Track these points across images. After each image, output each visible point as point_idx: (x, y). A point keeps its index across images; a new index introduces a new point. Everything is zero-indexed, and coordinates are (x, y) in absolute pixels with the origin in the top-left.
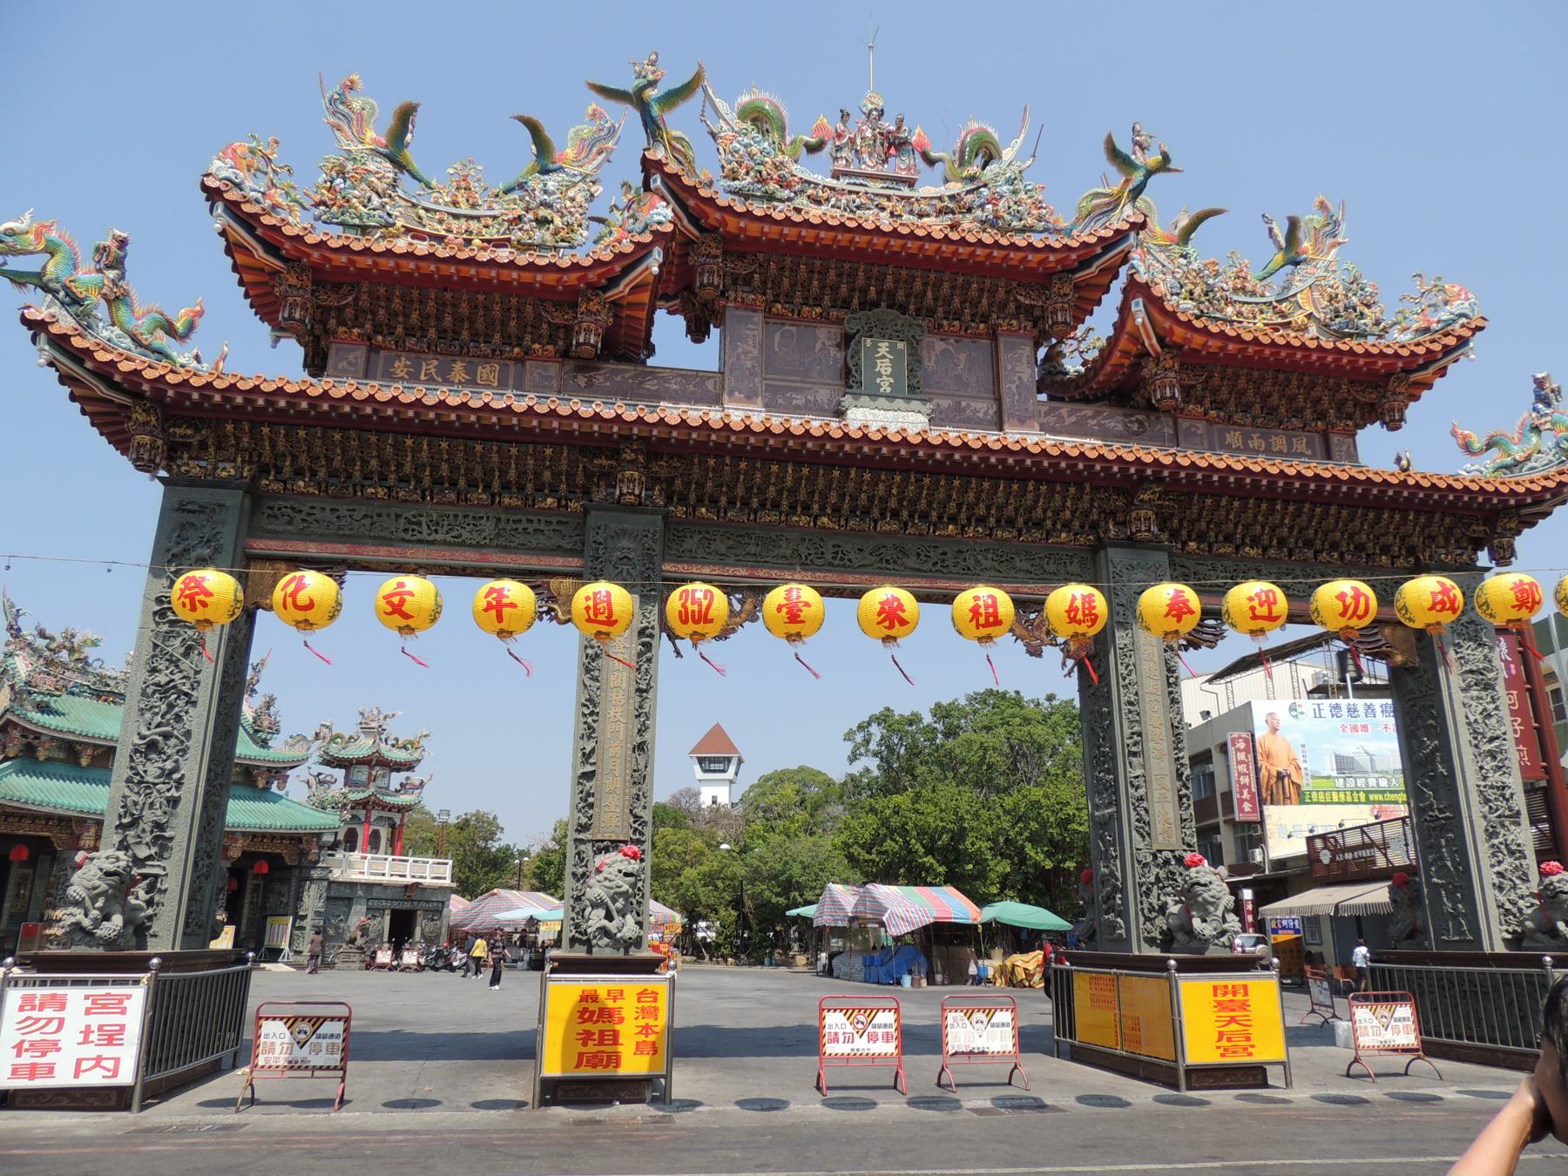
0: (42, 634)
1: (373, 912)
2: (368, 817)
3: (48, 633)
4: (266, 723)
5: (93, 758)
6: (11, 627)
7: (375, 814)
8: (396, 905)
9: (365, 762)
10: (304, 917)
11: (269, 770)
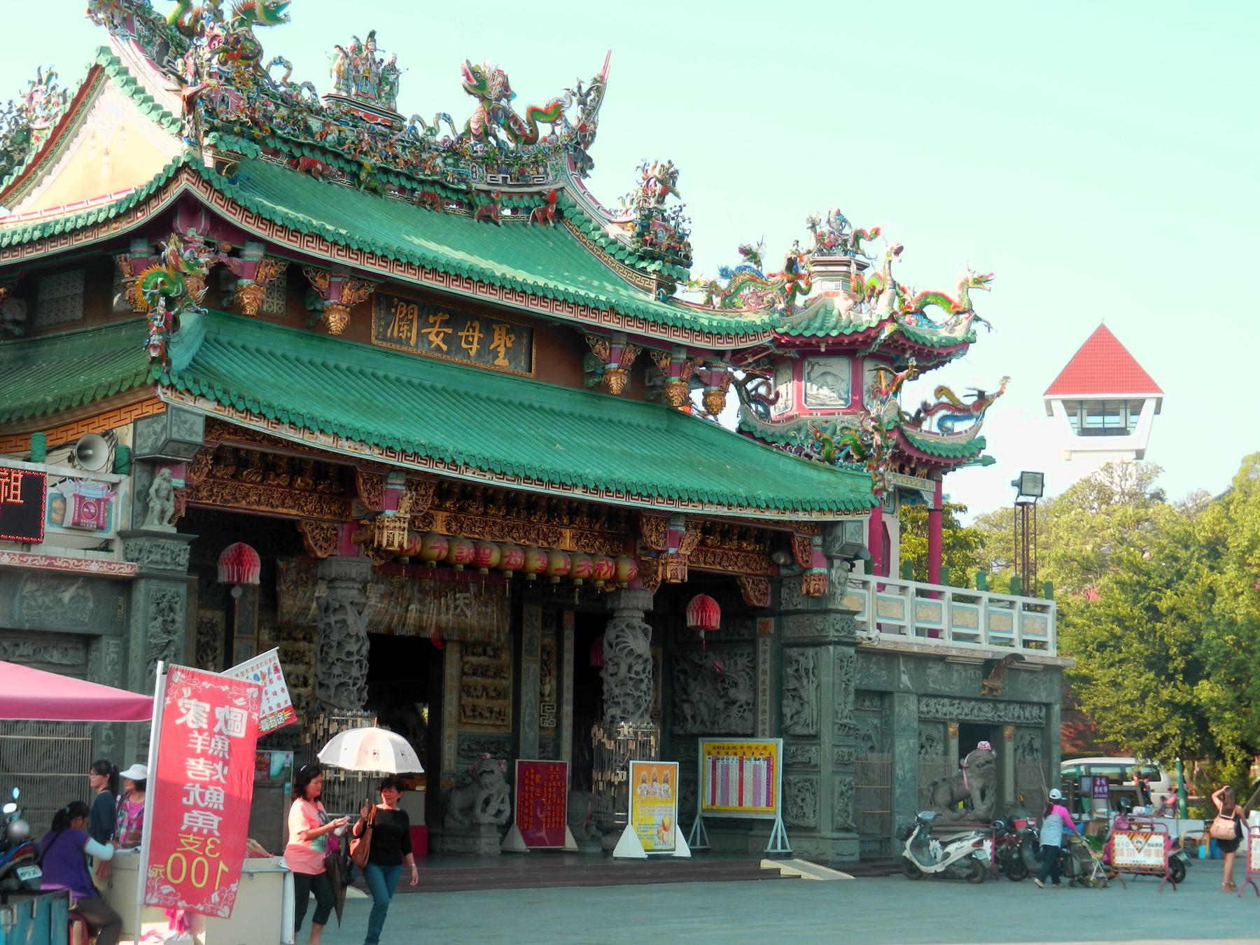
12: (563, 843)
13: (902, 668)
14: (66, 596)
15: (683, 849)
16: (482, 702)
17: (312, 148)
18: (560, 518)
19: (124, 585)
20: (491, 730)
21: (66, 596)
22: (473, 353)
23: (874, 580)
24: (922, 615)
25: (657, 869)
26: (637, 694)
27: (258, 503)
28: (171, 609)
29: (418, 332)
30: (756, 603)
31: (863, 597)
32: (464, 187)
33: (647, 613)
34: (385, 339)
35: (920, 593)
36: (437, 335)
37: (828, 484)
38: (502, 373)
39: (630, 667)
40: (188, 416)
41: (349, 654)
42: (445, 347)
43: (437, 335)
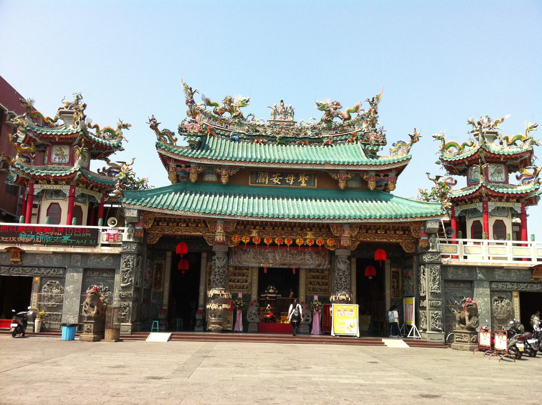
0: (208, 103)
1: (498, 294)
2: (485, 209)
3: (212, 101)
4: (372, 138)
5: (230, 177)
6: (187, 102)
7: (492, 205)
9: (473, 161)
10: (424, 298)
13: (478, 271)
14: (104, 259)
15: (358, 335)
16: (317, 286)
18: (306, 229)
19: (119, 256)
20: (323, 295)
21: (104, 259)
22: (291, 184)
23: (461, 241)
26: (340, 282)
28: (128, 261)
30: (407, 251)
31: (457, 247)
32: (317, 137)
34: (256, 183)
36: (276, 180)
37: (426, 208)
38: (303, 188)
41: (216, 272)
42: (280, 183)
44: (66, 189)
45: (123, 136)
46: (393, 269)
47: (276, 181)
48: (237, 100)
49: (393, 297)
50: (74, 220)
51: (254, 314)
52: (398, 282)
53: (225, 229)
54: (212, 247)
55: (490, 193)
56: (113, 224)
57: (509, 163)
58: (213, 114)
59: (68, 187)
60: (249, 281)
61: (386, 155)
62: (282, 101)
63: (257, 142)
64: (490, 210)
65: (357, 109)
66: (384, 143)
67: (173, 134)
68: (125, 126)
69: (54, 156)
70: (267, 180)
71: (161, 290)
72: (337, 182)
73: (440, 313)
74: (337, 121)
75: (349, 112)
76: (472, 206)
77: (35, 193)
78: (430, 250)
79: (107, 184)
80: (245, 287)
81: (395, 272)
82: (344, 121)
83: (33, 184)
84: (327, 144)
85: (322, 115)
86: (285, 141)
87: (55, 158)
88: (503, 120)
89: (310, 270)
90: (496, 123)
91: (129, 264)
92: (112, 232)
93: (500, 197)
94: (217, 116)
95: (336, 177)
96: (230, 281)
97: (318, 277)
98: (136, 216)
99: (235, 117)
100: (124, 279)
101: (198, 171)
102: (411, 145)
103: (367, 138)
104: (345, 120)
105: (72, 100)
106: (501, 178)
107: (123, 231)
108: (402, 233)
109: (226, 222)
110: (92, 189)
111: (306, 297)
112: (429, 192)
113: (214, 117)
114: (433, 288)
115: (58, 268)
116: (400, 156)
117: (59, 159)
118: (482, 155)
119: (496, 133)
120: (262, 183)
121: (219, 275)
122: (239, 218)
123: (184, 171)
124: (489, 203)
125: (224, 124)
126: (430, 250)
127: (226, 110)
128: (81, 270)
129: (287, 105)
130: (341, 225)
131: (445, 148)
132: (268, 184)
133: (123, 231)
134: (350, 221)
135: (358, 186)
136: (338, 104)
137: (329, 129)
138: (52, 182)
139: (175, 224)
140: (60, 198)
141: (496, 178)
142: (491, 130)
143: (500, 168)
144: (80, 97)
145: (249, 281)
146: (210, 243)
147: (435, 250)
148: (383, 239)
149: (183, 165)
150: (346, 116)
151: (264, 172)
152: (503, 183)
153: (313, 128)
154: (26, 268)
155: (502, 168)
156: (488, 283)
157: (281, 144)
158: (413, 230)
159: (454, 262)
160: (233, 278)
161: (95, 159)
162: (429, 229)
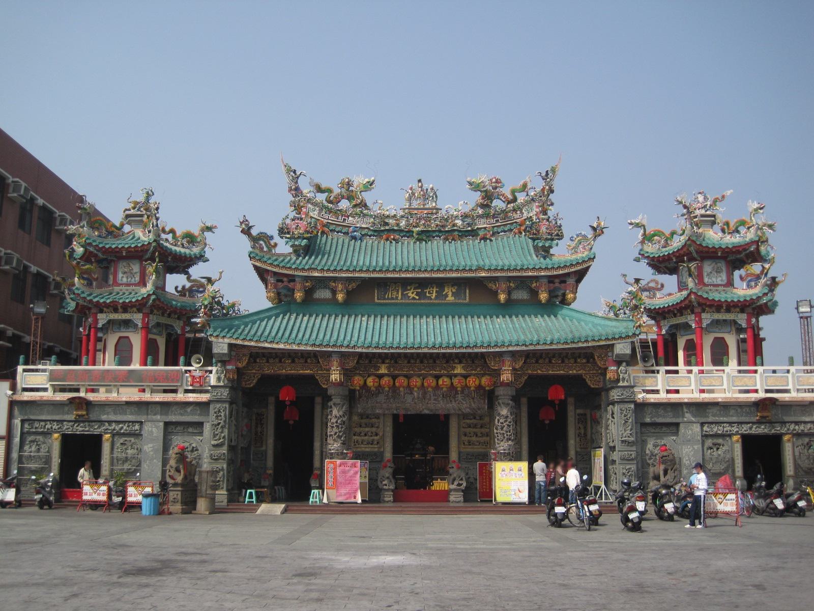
0: (319, 189)
2: (699, 322)
3: (323, 186)
4: (543, 229)
5: (349, 294)
6: (290, 190)
8: (745, 430)
11: (551, 279)
12: (700, 496)
13: (685, 410)
16: (474, 439)
17: (388, 231)
18: (453, 360)
22: (433, 298)
24: (705, 382)
25: (511, 508)
27: (291, 370)
28: (219, 411)
29: (402, 294)
30: (592, 386)
32: (470, 229)
33: (513, 396)
34: (385, 299)
35: (668, 372)
36: (413, 293)
37: (615, 327)
39: (499, 421)
40: (221, 344)
43: (413, 293)
44: (138, 318)
45: (208, 242)
46: (578, 411)
47: (411, 294)
48: (359, 180)
49: (578, 450)
50: (149, 359)
51: (388, 478)
52: (585, 428)
53: (342, 365)
54: (326, 389)
55: (704, 302)
56: (199, 363)
57: (731, 258)
58: (326, 204)
59: (140, 316)
60: (381, 434)
61: (562, 253)
62: (420, 181)
63: (387, 239)
64: (704, 325)
65: (524, 187)
66: (560, 237)
67: (272, 238)
68: (209, 229)
69: (120, 275)
70: (400, 294)
71: (264, 448)
72: (496, 294)
73: (634, 467)
74: (498, 204)
75: (513, 192)
76: (680, 320)
77: (100, 325)
78: (621, 384)
79: (188, 309)
80: (376, 443)
81: (582, 414)
82: (508, 203)
83: (96, 314)
84: (484, 239)
85: (477, 197)
86: (426, 236)
87: (122, 277)
88: (723, 197)
89: (465, 416)
90: (715, 202)
91: (221, 416)
92: (197, 374)
93: (718, 306)
94: (330, 205)
95: (494, 287)
96: (354, 435)
97: (475, 426)
98: (226, 351)
99: (355, 206)
100: (215, 435)
101: (305, 287)
102: (594, 240)
103: (536, 230)
104: (509, 202)
105: (141, 198)
106: (722, 278)
107: (211, 372)
108: (584, 361)
109: (344, 356)
110: (169, 316)
111: (460, 453)
112: (618, 304)
113: (326, 208)
114: (624, 435)
115: (133, 422)
116: (582, 255)
117: (127, 278)
118: (692, 249)
119: (714, 216)
120: (392, 299)
121: (337, 427)
122: (360, 350)
123: (286, 288)
124: (704, 315)
125: (340, 217)
126: (621, 384)
127: (343, 197)
128: (162, 424)
129: (428, 186)
130: (501, 354)
131: (647, 238)
132: (402, 299)
133: (211, 372)
134: (511, 349)
135: (525, 297)
136: (498, 181)
137: (486, 216)
138: (120, 310)
139: (277, 360)
140: (131, 329)
141: (714, 279)
142: (708, 213)
143: (719, 265)
144: (150, 192)
145: (381, 434)
146: (324, 384)
147: (625, 384)
148: (560, 371)
149: (285, 279)
150: (510, 197)
151: (395, 283)
152: (724, 286)
153: (465, 216)
154: (93, 424)
155: (722, 265)
156: (699, 425)
157: (420, 240)
158: (598, 357)
159: (652, 398)
160: (357, 430)
161: (171, 273)
162: (618, 355)
